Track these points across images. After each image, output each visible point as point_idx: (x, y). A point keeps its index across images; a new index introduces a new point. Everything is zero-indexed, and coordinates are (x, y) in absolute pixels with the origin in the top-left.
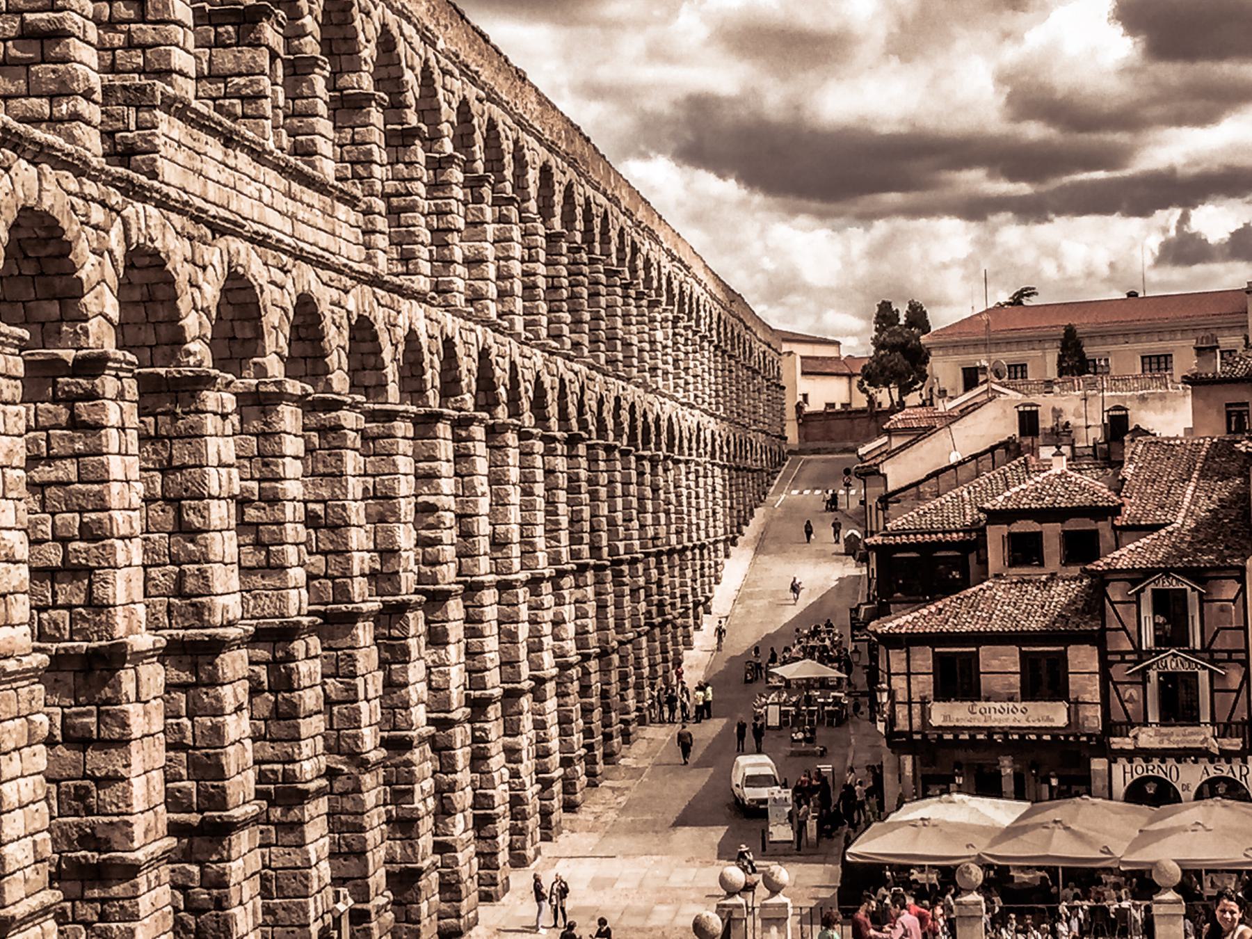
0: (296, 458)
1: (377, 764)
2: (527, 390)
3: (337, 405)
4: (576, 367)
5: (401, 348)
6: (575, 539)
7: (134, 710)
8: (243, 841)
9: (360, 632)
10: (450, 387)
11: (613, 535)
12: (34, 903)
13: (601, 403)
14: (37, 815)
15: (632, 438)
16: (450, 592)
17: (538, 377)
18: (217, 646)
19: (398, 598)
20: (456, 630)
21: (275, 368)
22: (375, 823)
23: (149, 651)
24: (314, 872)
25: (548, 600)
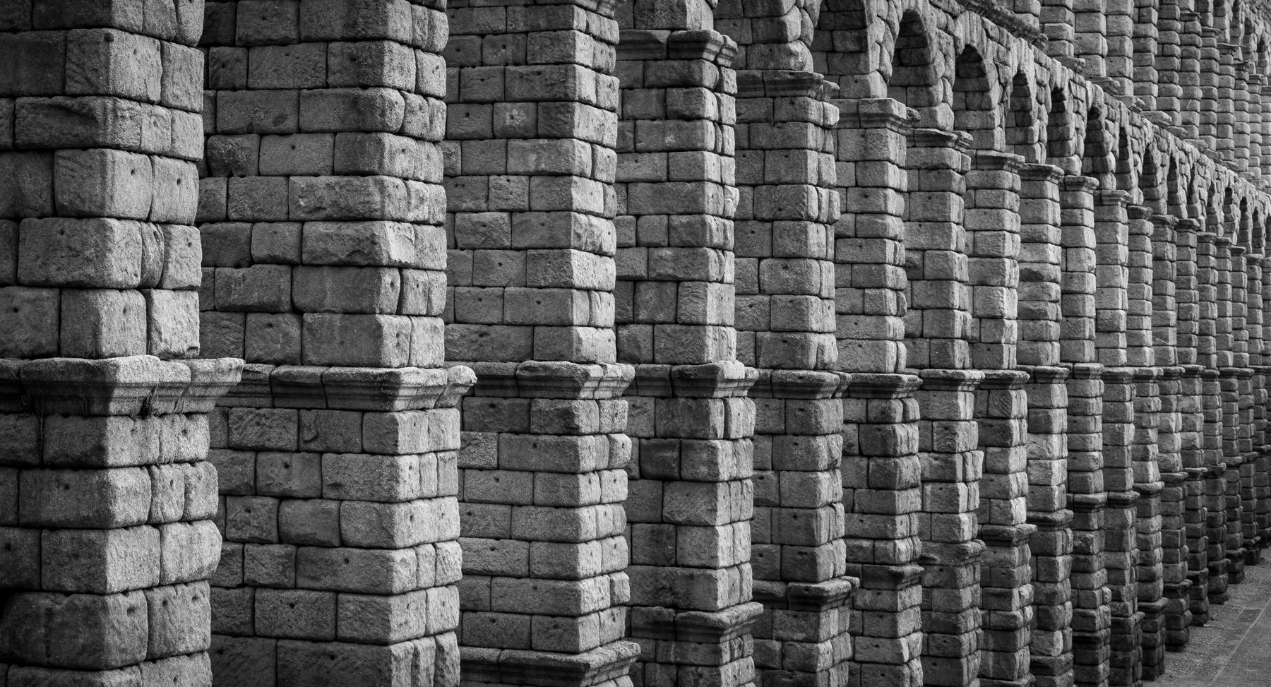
0: (898, 191)
1: (976, 555)
2: (1135, 164)
3: (940, 141)
4: (1188, 146)
5: (1009, 89)
6: (1183, 340)
7: (723, 447)
8: (833, 621)
9: (961, 402)
10: (1057, 145)
11: (1222, 345)
12: (609, 654)
13: (1211, 191)
14: (615, 552)
15: (1242, 239)
16: (1053, 373)
17: (1148, 152)
18: (810, 390)
19: (1000, 372)
20: (1060, 419)
21: (879, 89)
22: (971, 624)
23: (739, 381)
24: (906, 670)
25: (1156, 403)
